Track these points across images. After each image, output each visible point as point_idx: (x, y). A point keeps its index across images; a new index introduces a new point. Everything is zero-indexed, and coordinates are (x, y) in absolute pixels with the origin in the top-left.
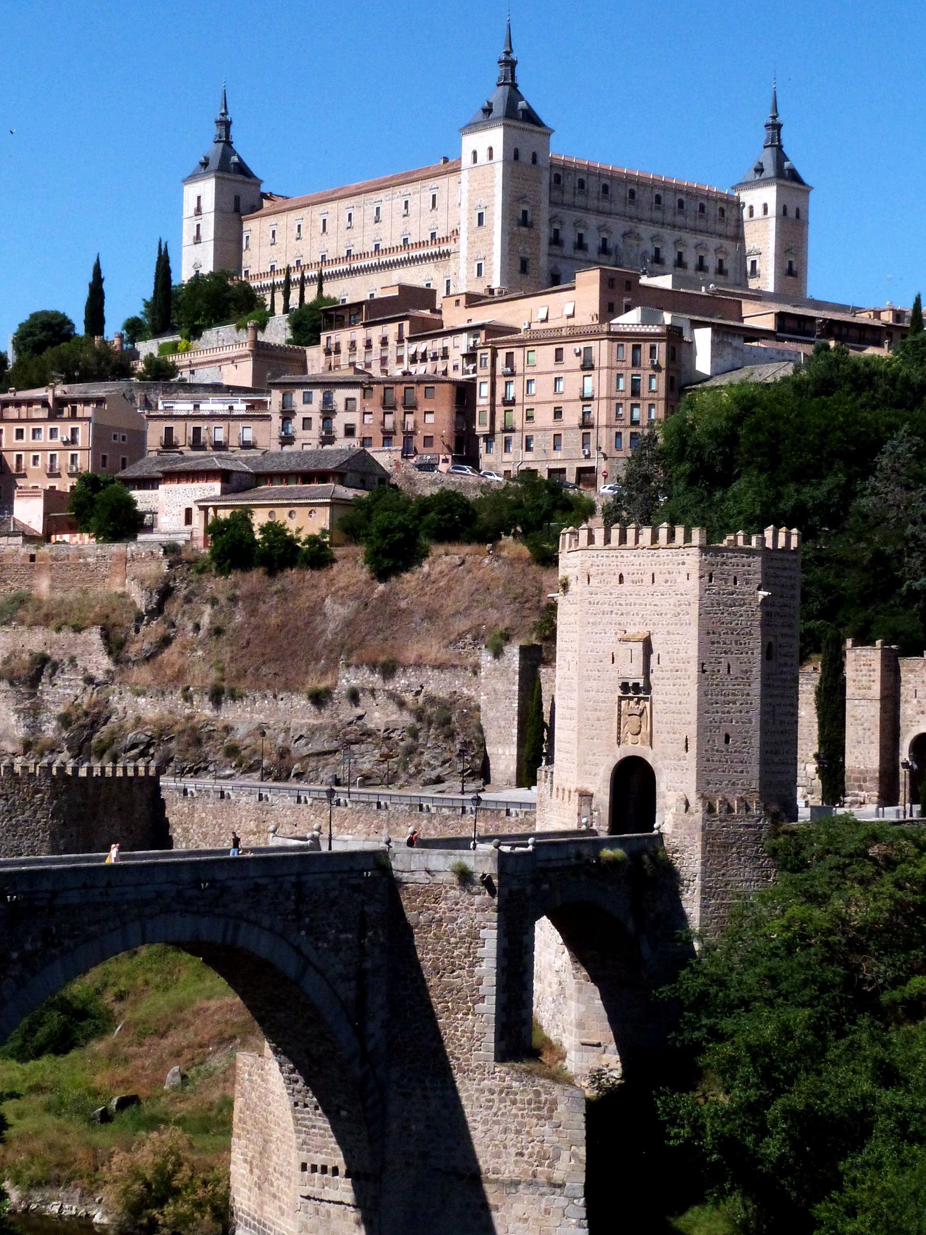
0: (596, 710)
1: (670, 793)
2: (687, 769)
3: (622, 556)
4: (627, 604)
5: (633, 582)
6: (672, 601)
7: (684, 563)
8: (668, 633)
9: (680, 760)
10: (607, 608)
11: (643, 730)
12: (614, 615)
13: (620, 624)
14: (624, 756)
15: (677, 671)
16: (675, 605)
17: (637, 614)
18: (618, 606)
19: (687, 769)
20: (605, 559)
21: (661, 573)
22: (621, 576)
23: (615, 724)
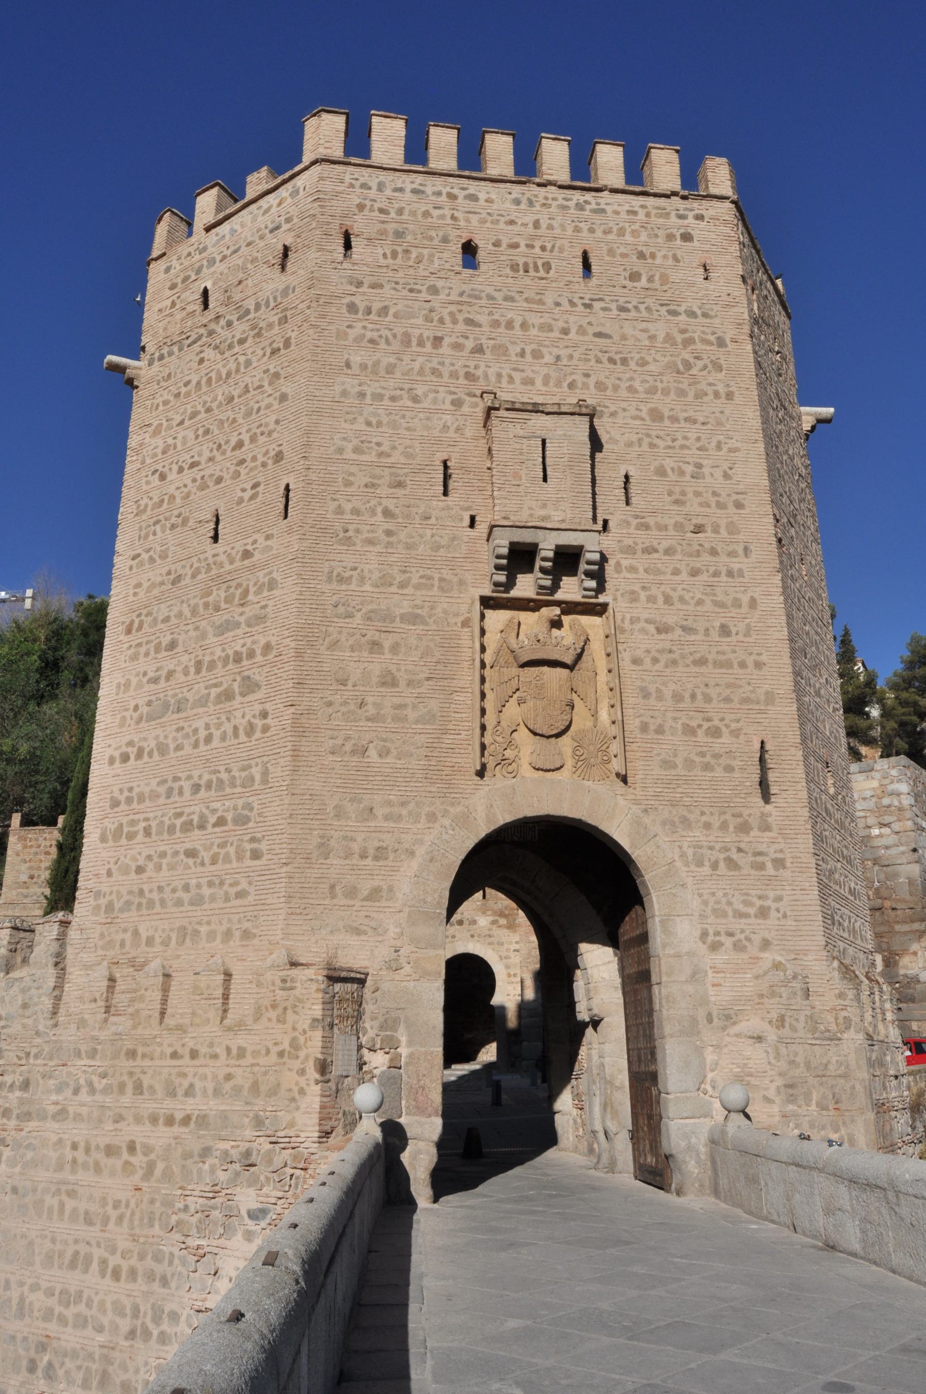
0: (375, 645)
1: (720, 958)
2: (779, 863)
3: (473, 198)
4: (496, 324)
5: (514, 268)
6: (660, 329)
7: (687, 237)
8: (656, 415)
9: (744, 828)
10: (419, 327)
11: (581, 720)
12: (445, 349)
13: (469, 376)
14: (503, 817)
15: (698, 530)
16: (669, 338)
17: (537, 355)
18: (461, 327)
19: (779, 863)
20: (408, 195)
21: (611, 252)
22: (469, 250)
23: (468, 699)
